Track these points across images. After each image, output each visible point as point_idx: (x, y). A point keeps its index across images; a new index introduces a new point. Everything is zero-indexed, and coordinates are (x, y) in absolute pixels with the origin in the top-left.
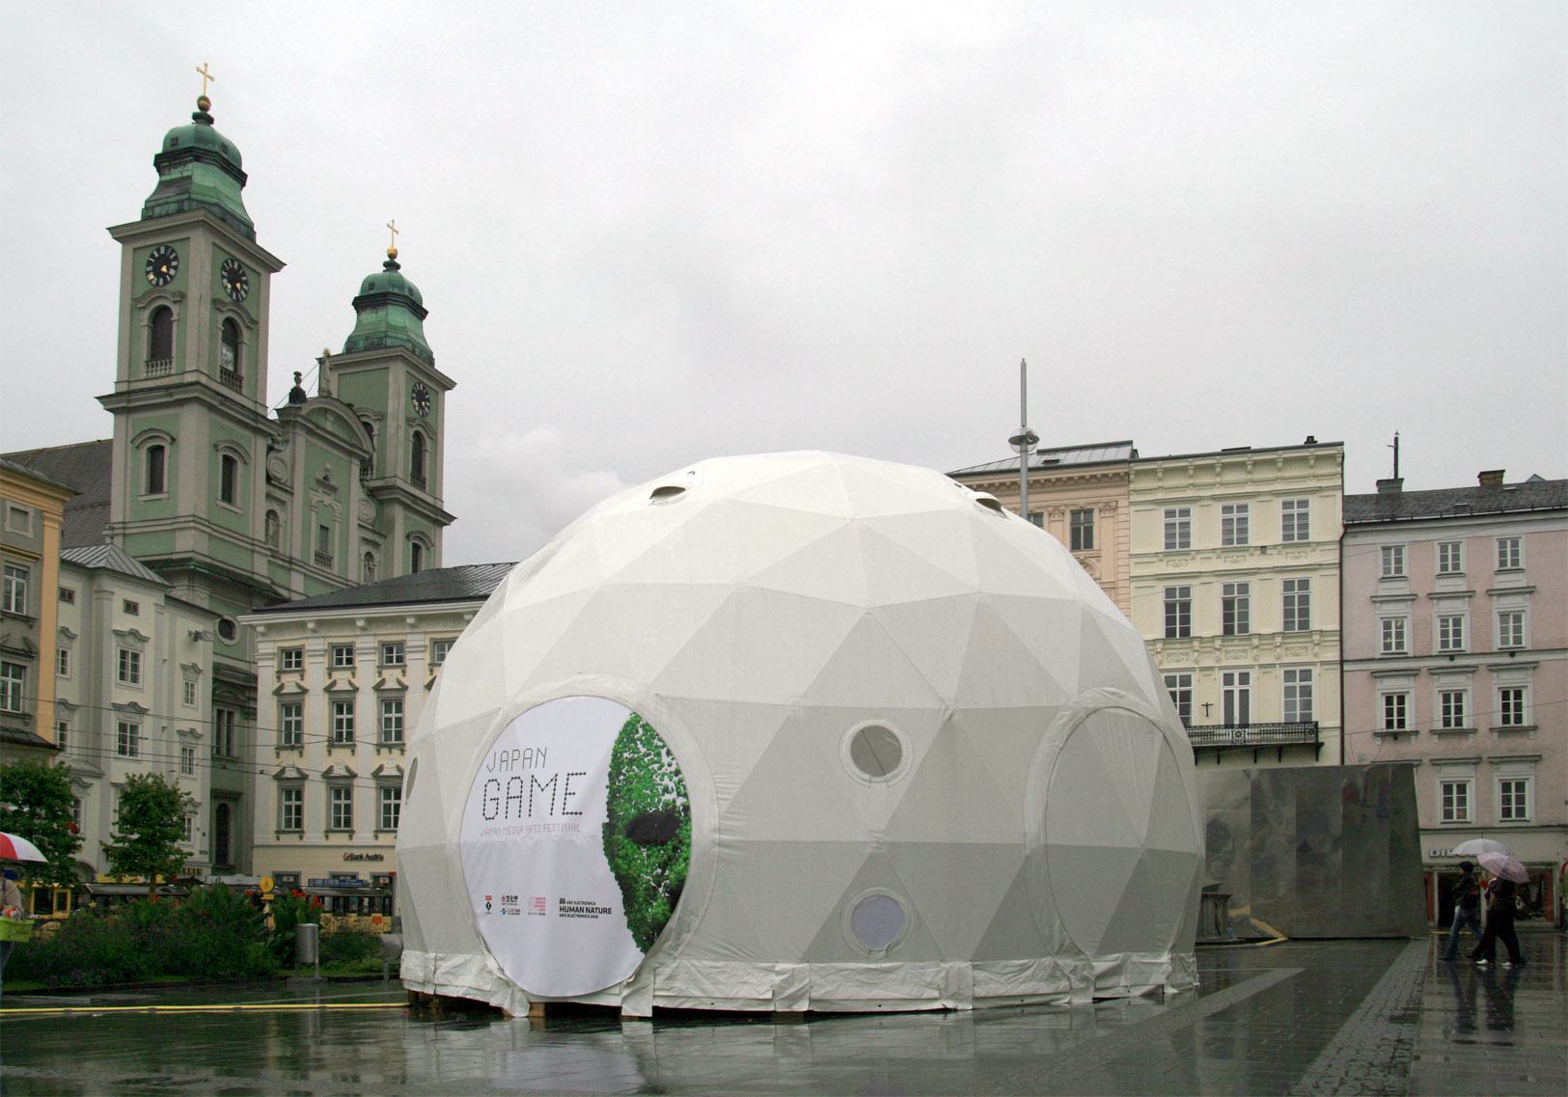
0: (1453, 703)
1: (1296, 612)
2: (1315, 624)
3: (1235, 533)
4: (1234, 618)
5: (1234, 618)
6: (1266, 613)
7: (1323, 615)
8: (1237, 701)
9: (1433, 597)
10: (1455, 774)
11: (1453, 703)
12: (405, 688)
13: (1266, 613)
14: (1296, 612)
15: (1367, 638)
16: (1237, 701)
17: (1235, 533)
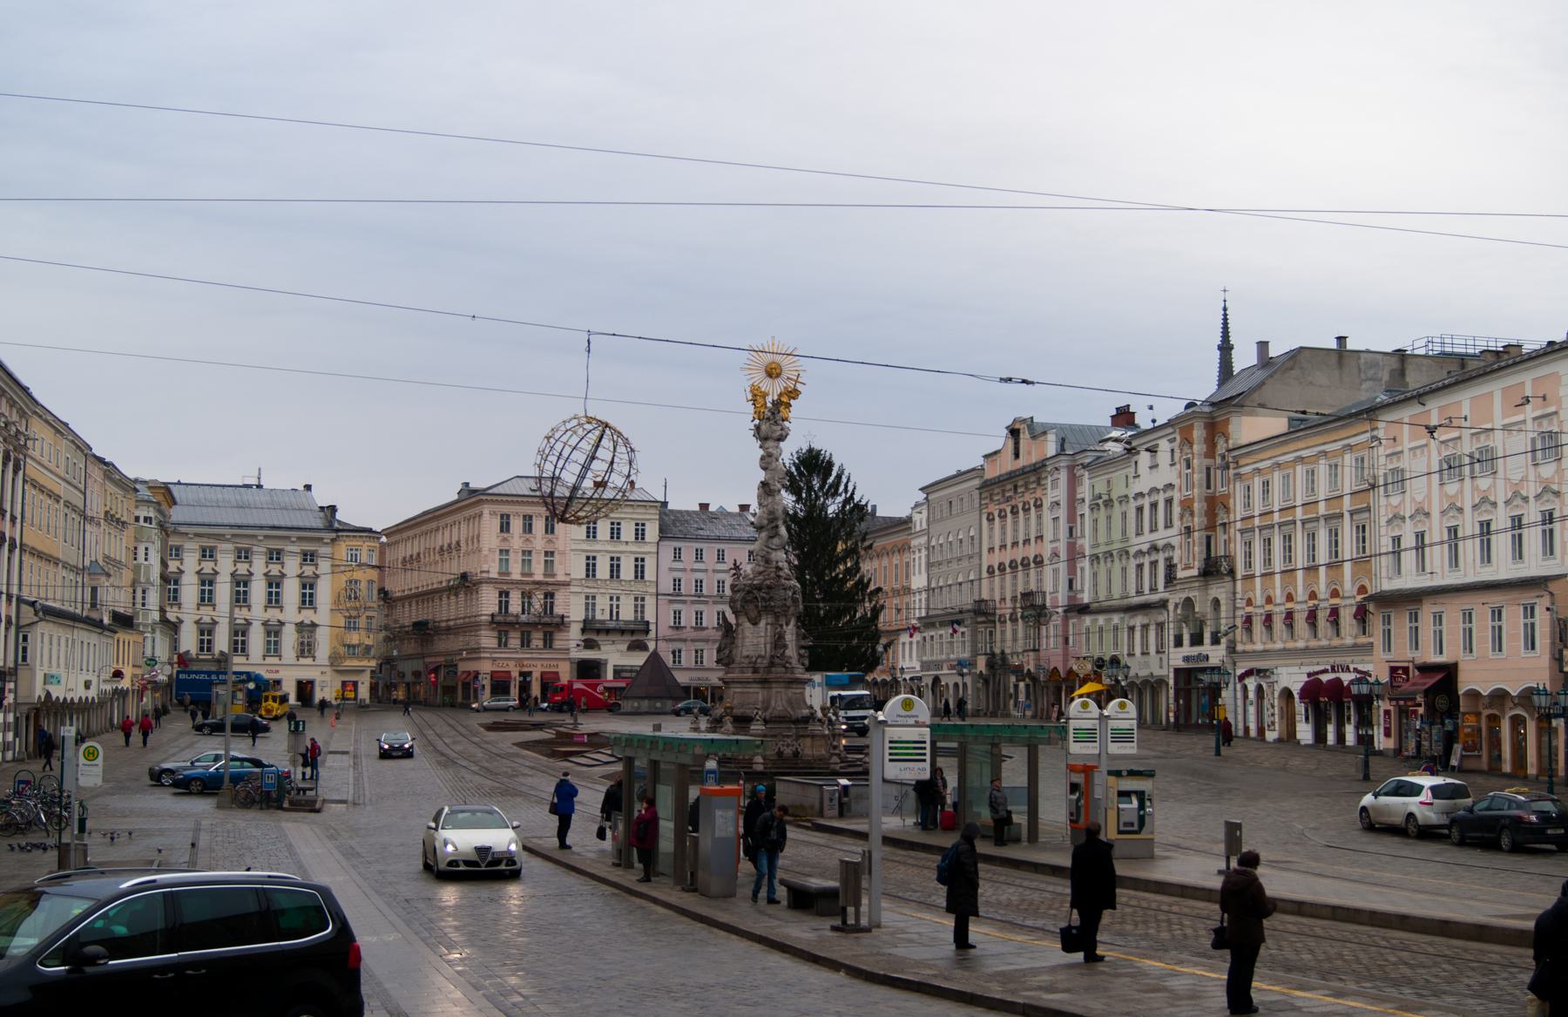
0: (699, 615)
1: (640, 572)
2: (647, 577)
3: (615, 534)
4: (615, 570)
5: (615, 570)
6: (627, 571)
7: (649, 574)
8: (614, 612)
9: (693, 570)
10: (699, 645)
11: (699, 615)
12: (181, 572)
13: (627, 571)
14: (640, 572)
15: (667, 586)
16: (614, 612)
17: (615, 534)
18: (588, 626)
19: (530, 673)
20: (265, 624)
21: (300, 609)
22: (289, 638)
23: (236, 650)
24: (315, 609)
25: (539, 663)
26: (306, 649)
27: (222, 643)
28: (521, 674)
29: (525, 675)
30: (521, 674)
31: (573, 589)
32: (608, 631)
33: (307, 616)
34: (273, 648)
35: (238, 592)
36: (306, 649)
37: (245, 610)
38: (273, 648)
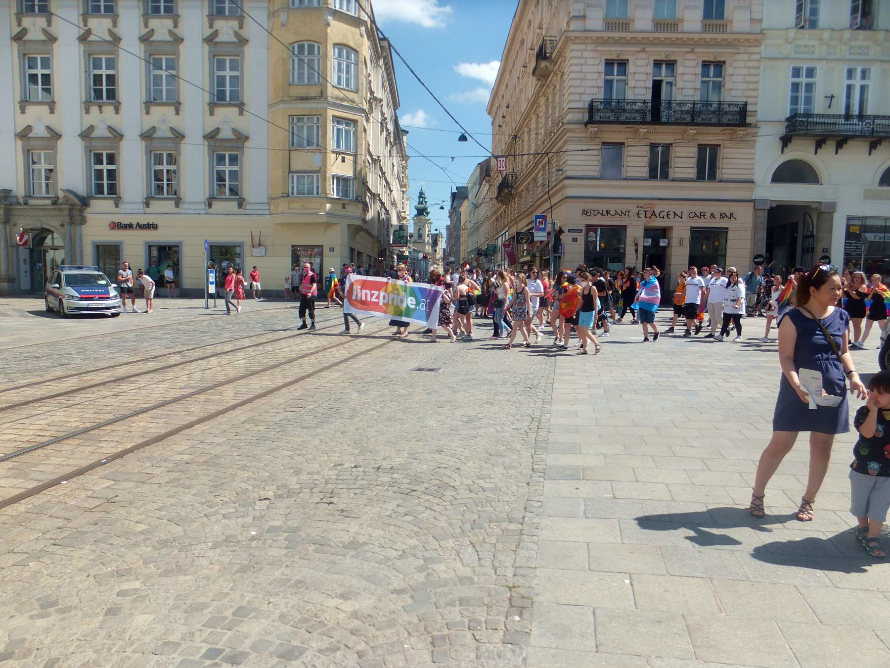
18: (796, 127)
19: (664, 232)
20: (148, 136)
21: (212, 106)
22: (194, 170)
23: (100, 189)
24: (241, 107)
25: (686, 208)
26: (226, 186)
27: (72, 171)
28: (649, 232)
29: (657, 234)
30: (649, 232)
31: (763, 50)
32: (841, 142)
33: (227, 119)
34: (163, 185)
35: (97, 79)
36: (226, 186)
37: (109, 110)
38: (163, 185)
